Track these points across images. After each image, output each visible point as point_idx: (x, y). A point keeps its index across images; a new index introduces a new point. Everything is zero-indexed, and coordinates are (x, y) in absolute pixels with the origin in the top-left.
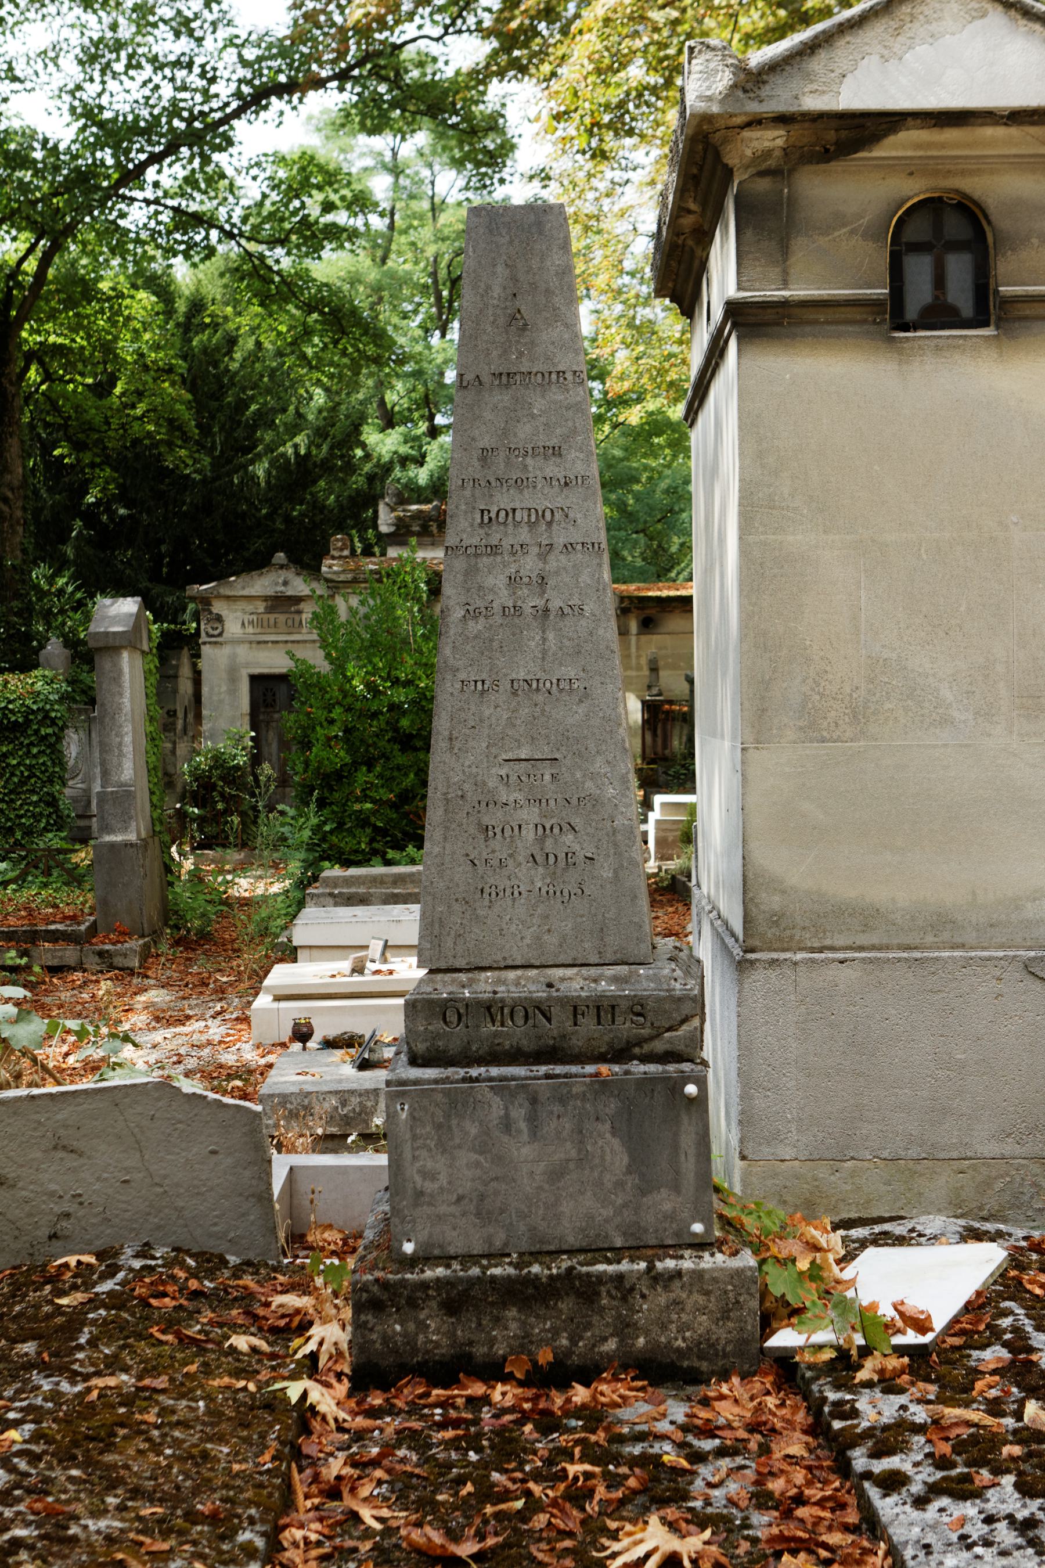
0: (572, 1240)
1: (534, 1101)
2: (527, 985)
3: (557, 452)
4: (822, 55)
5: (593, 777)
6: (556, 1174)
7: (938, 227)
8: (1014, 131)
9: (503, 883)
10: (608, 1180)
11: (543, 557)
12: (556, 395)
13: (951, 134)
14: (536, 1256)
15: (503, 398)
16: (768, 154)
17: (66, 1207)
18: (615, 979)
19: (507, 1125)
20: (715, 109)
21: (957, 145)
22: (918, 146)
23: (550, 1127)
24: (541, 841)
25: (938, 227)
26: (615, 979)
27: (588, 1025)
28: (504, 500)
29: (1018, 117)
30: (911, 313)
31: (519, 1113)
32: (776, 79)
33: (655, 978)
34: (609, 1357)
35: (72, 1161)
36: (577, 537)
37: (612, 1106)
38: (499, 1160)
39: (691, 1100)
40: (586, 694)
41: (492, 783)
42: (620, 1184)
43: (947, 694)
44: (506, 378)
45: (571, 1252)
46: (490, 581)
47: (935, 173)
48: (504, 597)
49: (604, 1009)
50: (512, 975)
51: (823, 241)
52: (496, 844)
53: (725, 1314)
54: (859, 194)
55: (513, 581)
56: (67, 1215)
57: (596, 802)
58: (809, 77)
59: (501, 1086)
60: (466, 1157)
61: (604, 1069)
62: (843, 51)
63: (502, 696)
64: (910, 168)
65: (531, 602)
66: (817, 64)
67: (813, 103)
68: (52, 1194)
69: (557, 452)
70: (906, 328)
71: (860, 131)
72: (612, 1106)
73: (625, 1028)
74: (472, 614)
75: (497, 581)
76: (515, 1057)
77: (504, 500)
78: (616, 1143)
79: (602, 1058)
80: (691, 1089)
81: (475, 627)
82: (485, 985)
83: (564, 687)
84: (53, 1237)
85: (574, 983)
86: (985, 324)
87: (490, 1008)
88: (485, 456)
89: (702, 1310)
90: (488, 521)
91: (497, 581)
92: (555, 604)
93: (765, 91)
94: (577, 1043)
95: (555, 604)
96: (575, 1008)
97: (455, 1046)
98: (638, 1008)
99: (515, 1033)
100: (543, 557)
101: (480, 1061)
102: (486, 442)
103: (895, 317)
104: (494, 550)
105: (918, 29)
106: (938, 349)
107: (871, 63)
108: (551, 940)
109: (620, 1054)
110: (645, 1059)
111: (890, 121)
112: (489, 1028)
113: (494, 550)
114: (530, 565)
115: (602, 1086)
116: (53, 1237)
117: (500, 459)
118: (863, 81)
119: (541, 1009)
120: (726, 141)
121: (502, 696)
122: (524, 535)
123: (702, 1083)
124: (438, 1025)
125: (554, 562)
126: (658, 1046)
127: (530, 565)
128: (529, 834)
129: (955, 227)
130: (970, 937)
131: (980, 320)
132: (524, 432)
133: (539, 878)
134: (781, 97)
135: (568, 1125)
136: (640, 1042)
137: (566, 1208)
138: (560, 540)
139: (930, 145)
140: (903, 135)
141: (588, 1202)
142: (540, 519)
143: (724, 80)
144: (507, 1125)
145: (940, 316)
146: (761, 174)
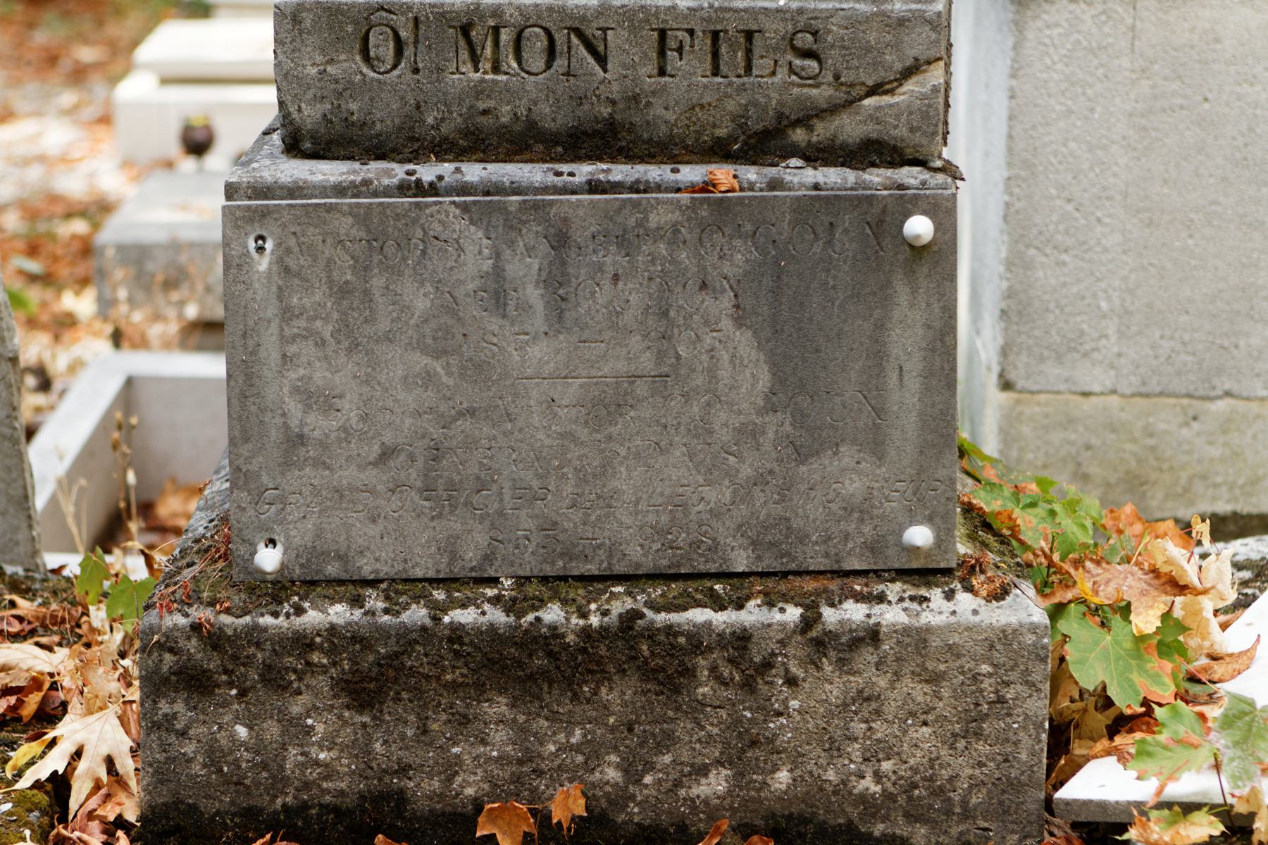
0: (637, 554)
1: (560, 240)
6: (606, 406)
14: (556, 584)
19: (497, 293)
23: (594, 301)
27: (690, 70)
31: (526, 267)
37: (740, 258)
38: (478, 370)
39: (918, 251)
42: (749, 433)
53: (972, 727)
59: (484, 204)
60: (402, 362)
61: (723, 174)
73: (776, 84)
76: (523, 141)
78: (744, 341)
79: (720, 151)
80: (919, 227)
89: (922, 715)
94: (665, 115)
97: (386, 115)
99: (526, 88)
101: (444, 149)
109: (762, 142)
110: (817, 156)
112: (464, 76)
115: (716, 210)
123: (944, 213)
124: (349, 65)
126: (850, 128)
135: (635, 296)
137: (626, 481)
141: (676, 470)
144: (497, 293)
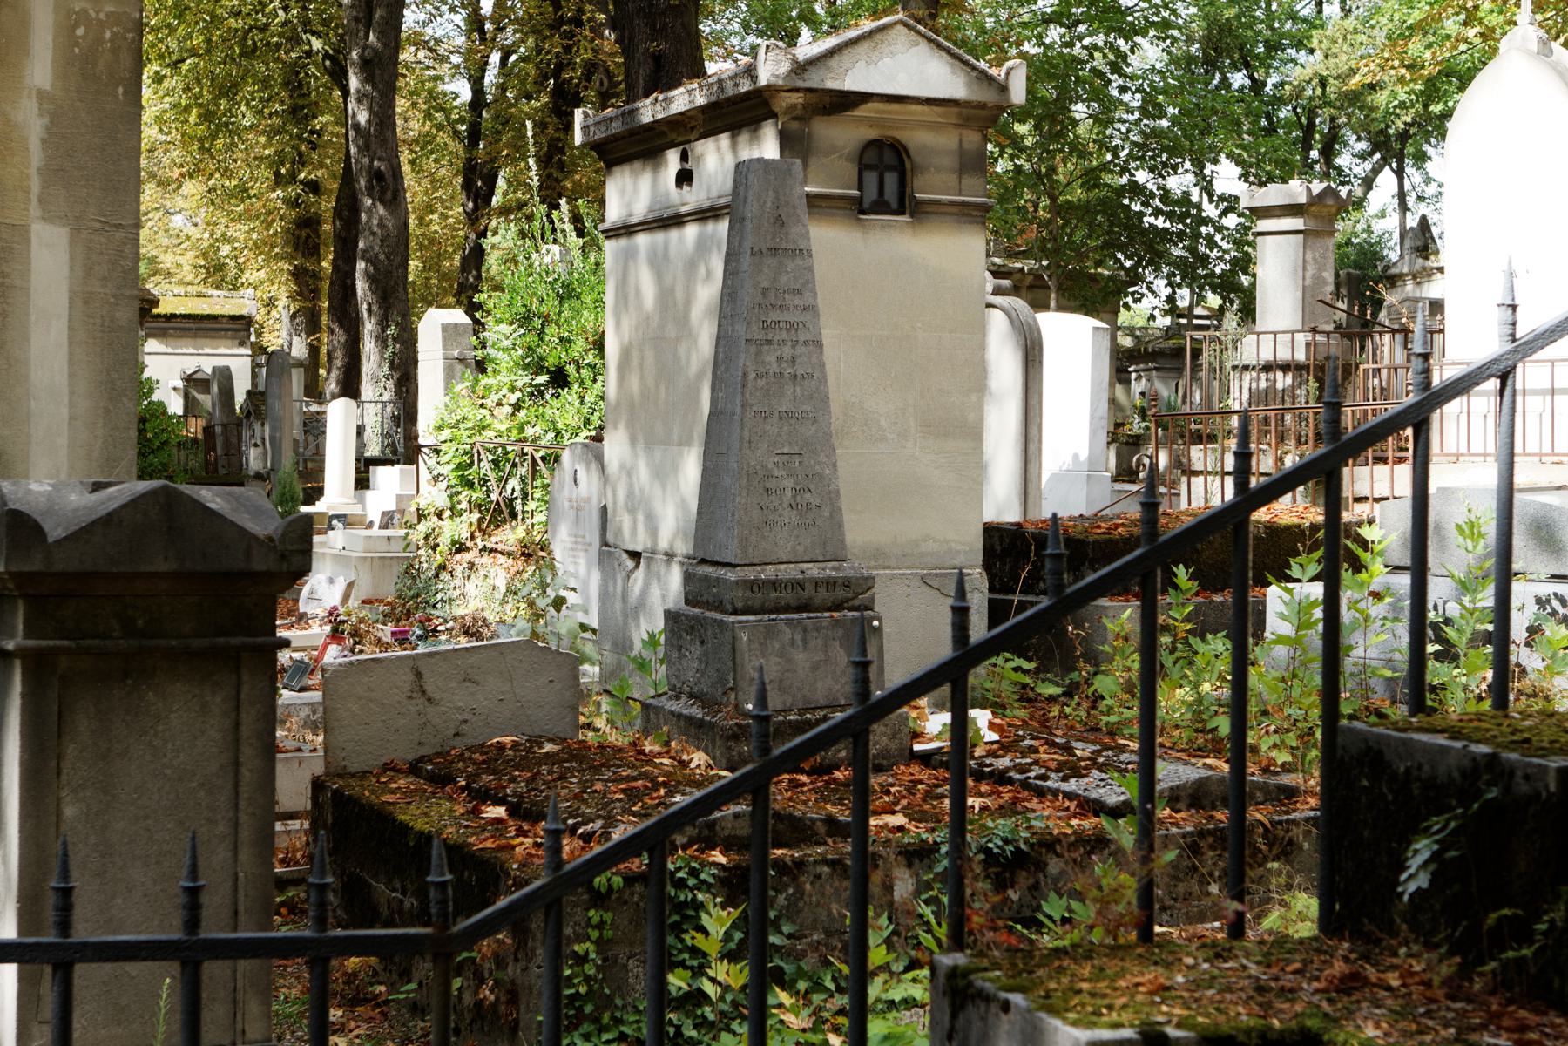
0: (822, 702)
1: (805, 630)
2: (788, 572)
3: (800, 292)
4: (836, 57)
5: (819, 463)
6: (815, 668)
7: (881, 156)
8: (926, 108)
9: (777, 519)
10: (839, 670)
11: (793, 347)
12: (799, 262)
13: (895, 107)
14: (806, 710)
15: (772, 261)
16: (794, 106)
17: (466, 716)
18: (833, 569)
19: (793, 643)
20: (780, 82)
21: (896, 113)
22: (877, 112)
23: (812, 644)
24: (794, 497)
25: (881, 156)
26: (833, 569)
27: (822, 591)
28: (774, 316)
29: (930, 102)
30: (866, 205)
31: (798, 637)
32: (812, 69)
33: (853, 568)
34: (843, 760)
35: (473, 688)
36: (809, 337)
37: (840, 632)
38: (789, 661)
39: (875, 629)
40: (815, 421)
41: (770, 466)
42: (844, 672)
43: (883, 423)
44: (774, 251)
45: (822, 708)
46: (768, 359)
47: (883, 127)
48: (774, 368)
49: (830, 584)
50: (782, 567)
51: (825, 160)
52: (773, 498)
53: (894, 736)
54: (843, 134)
55: (779, 359)
56: (466, 721)
57: (821, 476)
58: (829, 69)
59: (789, 622)
60: (774, 660)
61: (835, 614)
62: (847, 56)
63: (775, 419)
64: (871, 123)
65: (788, 371)
66: (833, 62)
67: (831, 84)
68: (459, 708)
69: (800, 292)
70: (864, 213)
71: (847, 101)
72: (840, 632)
73: (840, 593)
74: (759, 376)
75: (771, 359)
76: (787, 609)
77: (774, 316)
78: (842, 652)
79: (829, 610)
80: (876, 623)
81: (761, 383)
82: (769, 572)
83: (804, 416)
84: (457, 734)
85: (814, 571)
86: (903, 213)
87: (775, 584)
88: (765, 291)
89: (884, 734)
90: (766, 327)
91: (771, 359)
92: (800, 372)
93: (807, 75)
94: (817, 601)
95: (800, 372)
96: (817, 583)
97: (757, 604)
98: (847, 583)
99: (788, 597)
100: (793, 347)
101: (771, 612)
102: (765, 284)
103: (858, 208)
104: (770, 342)
105: (885, 48)
106: (883, 227)
107: (861, 64)
108: (800, 549)
109: (838, 607)
110: (850, 609)
111: (864, 97)
112: (774, 595)
113: (770, 342)
114: (787, 351)
115: (836, 623)
116: (457, 734)
117: (772, 294)
118: (856, 76)
119: (800, 584)
120: (772, 96)
121: (775, 419)
122: (784, 335)
123: (880, 619)
124: (748, 593)
125: (800, 349)
126: (856, 603)
127: (787, 351)
128: (789, 493)
129: (889, 157)
130: (893, 562)
131: (901, 211)
132: (783, 279)
133: (794, 516)
134: (815, 80)
135: (820, 642)
136: (848, 600)
137: (819, 685)
138: (802, 339)
139: (884, 112)
140: (870, 105)
141: (829, 682)
142: (792, 327)
143: (786, 67)
144: (793, 643)
145: (880, 207)
146: (794, 119)
